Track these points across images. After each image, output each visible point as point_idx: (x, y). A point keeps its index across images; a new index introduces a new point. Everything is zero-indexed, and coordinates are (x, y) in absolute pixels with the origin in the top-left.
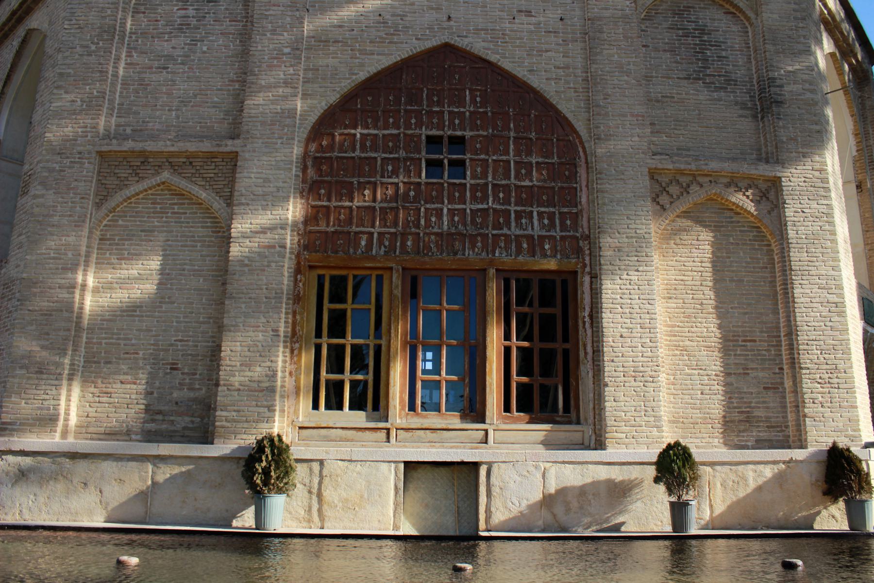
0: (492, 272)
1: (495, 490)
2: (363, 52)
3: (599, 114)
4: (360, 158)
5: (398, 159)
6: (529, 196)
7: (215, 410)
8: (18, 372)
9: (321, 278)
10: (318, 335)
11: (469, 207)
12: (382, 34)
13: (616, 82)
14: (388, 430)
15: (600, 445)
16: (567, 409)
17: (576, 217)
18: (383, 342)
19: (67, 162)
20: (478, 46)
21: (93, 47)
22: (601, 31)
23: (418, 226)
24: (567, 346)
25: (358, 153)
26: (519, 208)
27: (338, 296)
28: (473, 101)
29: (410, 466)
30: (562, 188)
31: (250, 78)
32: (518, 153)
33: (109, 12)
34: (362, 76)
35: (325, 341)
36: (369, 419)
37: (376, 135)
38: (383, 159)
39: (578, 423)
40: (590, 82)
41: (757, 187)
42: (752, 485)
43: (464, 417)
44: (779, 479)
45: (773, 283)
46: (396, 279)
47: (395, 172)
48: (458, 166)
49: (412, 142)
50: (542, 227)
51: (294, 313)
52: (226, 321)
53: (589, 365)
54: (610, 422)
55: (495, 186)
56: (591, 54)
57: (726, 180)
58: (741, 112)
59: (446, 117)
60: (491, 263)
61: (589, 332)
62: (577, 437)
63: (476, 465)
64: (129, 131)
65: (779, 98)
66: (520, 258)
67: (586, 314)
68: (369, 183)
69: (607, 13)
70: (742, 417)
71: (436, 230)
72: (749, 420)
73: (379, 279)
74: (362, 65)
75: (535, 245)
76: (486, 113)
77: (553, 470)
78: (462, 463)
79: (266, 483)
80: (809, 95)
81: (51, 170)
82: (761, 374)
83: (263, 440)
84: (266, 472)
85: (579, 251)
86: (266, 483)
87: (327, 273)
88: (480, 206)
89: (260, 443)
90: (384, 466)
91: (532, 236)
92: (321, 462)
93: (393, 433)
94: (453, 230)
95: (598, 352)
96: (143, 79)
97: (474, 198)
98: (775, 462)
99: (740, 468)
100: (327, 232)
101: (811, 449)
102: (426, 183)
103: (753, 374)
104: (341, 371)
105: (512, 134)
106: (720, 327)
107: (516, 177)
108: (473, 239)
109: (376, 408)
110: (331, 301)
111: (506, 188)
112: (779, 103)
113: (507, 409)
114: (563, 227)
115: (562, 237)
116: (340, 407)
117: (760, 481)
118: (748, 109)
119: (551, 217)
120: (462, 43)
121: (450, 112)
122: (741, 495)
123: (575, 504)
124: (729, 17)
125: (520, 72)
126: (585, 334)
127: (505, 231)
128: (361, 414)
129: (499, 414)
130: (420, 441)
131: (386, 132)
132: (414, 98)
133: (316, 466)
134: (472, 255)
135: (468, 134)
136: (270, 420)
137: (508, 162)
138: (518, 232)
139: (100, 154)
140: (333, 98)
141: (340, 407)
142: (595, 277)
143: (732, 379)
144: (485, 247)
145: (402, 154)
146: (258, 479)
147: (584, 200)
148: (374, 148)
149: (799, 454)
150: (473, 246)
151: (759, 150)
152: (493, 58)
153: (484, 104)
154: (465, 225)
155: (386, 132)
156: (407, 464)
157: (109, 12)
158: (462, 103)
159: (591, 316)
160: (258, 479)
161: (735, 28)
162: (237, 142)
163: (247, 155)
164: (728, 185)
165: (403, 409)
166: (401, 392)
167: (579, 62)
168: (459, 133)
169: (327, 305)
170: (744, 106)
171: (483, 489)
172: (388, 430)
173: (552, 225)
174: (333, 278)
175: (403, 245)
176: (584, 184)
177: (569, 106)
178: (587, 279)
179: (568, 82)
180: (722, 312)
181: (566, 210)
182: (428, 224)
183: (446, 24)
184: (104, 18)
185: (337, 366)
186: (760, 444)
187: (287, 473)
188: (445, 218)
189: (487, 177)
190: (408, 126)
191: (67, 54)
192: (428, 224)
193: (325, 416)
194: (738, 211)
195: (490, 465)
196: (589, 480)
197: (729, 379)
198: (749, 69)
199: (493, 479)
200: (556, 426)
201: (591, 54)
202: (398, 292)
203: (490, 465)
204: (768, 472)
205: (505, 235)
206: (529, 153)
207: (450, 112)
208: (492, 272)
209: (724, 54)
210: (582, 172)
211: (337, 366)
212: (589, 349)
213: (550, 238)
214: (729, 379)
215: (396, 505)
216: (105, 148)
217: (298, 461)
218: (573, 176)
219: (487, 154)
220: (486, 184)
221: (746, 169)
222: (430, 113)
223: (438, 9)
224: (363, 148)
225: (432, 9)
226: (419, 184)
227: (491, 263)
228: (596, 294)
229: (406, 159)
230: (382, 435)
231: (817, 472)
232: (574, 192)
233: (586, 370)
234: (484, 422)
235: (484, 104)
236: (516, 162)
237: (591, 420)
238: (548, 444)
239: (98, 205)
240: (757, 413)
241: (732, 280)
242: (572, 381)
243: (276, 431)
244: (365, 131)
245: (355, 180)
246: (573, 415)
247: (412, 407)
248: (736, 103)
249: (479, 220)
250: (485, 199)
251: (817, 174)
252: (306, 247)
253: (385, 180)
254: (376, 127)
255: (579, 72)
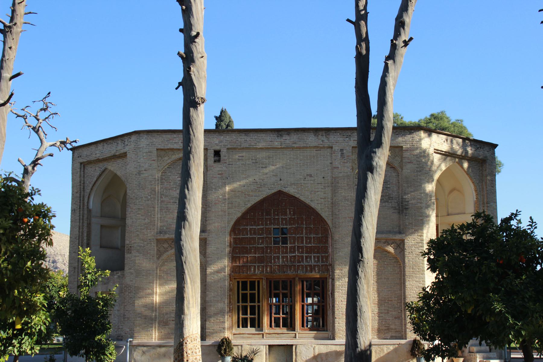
0: (297, 279)
1: (298, 354)
2: (249, 195)
3: (336, 218)
4: (250, 238)
5: (263, 238)
6: (310, 250)
7: (205, 329)
8: (138, 319)
9: (238, 282)
10: (238, 302)
11: (289, 255)
12: (256, 188)
13: (343, 204)
14: (263, 334)
15: (334, 339)
16: (323, 326)
17: (327, 258)
18: (260, 304)
19: (146, 243)
20: (291, 190)
21: (149, 197)
22: (338, 183)
23: (271, 263)
24: (323, 304)
25: (249, 236)
26: (307, 255)
27: (244, 288)
28: (290, 213)
29: (270, 346)
30: (322, 247)
31: (208, 209)
32: (306, 234)
33: (153, 182)
34: (249, 205)
35: (240, 304)
36: (256, 330)
37: (255, 229)
38: (258, 238)
39: (327, 331)
40: (333, 204)
41: (396, 243)
42: (386, 352)
43: (288, 330)
44: (395, 350)
45: (400, 279)
46: (264, 282)
47: (262, 243)
48: (285, 241)
49: (268, 231)
50: (315, 261)
51: (230, 295)
52: (207, 299)
53: (331, 311)
54: (337, 330)
55: (298, 247)
56: (334, 191)
57: (383, 241)
58: (393, 211)
59: (280, 220)
60: (297, 276)
61: (331, 299)
62: (326, 335)
63: (292, 345)
64: (165, 228)
65: (407, 207)
66: (307, 274)
67: (330, 293)
68: (253, 247)
69: (341, 175)
70: (386, 328)
71: (278, 264)
72: (388, 329)
73: (259, 282)
74: (249, 201)
75: (312, 268)
76: (295, 218)
77: (317, 347)
78: (287, 345)
79: (225, 353)
80: (419, 205)
81: (140, 246)
82: (394, 313)
83: (223, 339)
84: (225, 350)
85: (328, 270)
86: (225, 353)
87: (240, 280)
88: (293, 255)
89: (222, 340)
90: (262, 346)
91: (311, 265)
92: (242, 346)
93: (265, 335)
94: (283, 264)
95: (333, 306)
96: (167, 207)
97: (291, 252)
98: (394, 344)
99: (381, 346)
100: (239, 266)
101: (408, 340)
102: (274, 247)
103: (391, 313)
104: (247, 314)
105: (304, 226)
106: (378, 296)
107: (306, 243)
108: (290, 266)
109: (259, 326)
110: (242, 290)
111: (302, 248)
112: (406, 209)
113: (303, 326)
114: (322, 261)
115: (322, 265)
116: (247, 327)
117: (389, 351)
118: (396, 209)
119: (318, 257)
120: (285, 190)
121: (282, 218)
122: (382, 355)
123: (324, 358)
124: (392, 169)
125: (307, 201)
126: (330, 300)
127: (302, 264)
128: (254, 329)
129: (300, 328)
130: (273, 337)
131: (259, 227)
132: (268, 214)
133: (240, 347)
134: (290, 273)
135: (288, 227)
136: (224, 332)
137: (303, 237)
138: (306, 264)
139: (157, 239)
140: (239, 215)
141: (247, 327)
142: (333, 280)
143: (383, 315)
144: (295, 270)
145: (265, 235)
146: (223, 352)
147: (330, 251)
148: (255, 234)
149: (403, 342)
150: (290, 270)
151: (400, 226)
152: (297, 196)
153: (294, 214)
154: (287, 262)
155: (259, 227)
156: (269, 346)
157: (153, 182)
158: (286, 214)
159: (331, 294)
160: (223, 352)
161: (394, 174)
162: (206, 234)
163: (210, 239)
164: (385, 243)
165: (268, 327)
166: (267, 321)
167: (330, 195)
168: (285, 227)
169: (241, 292)
170: (395, 208)
171: (294, 353)
172: (263, 334)
173: (318, 260)
174: (242, 282)
175: (266, 270)
176: (330, 244)
177: (325, 214)
178: (330, 280)
179: (325, 205)
180: (379, 292)
181: (323, 255)
182: (275, 262)
183: (279, 182)
184: (152, 185)
185: (245, 313)
186: (392, 338)
187: (231, 350)
188: (281, 260)
189: (295, 244)
190: (266, 225)
191: (140, 200)
192: (275, 262)
193: (242, 330)
194: (389, 252)
195: (296, 345)
196: (329, 350)
197: (381, 315)
198: (398, 192)
199: (297, 350)
200: (319, 332)
201: (334, 191)
202: (265, 287)
203: (296, 345)
204: (392, 348)
205: (302, 265)
206: (310, 233)
207: (282, 218)
208: (297, 279)
209: (389, 186)
210: (330, 240)
211: (245, 313)
212: (331, 305)
213: (317, 265)
214: (381, 315)
215: (266, 359)
216: (159, 238)
217: (234, 345)
218: (326, 242)
219: (295, 234)
220: (295, 246)
221: (391, 237)
222: (274, 219)
223: (276, 176)
224: (251, 234)
225: (274, 176)
226: (271, 247)
227: (297, 276)
228: (333, 285)
229: (266, 238)
230: (261, 336)
231: (409, 348)
232: (327, 248)
233: (330, 312)
234: (295, 331)
235: (294, 214)
236: (306, 237)
237: (331, 330)
238: (316, 338)
239: (158, 258)
240: (391, 327)
241: (385, 278)
242: (325, 317)
243: (226, 336)
244: (251, 227)
245: (248, 246)
246: (325, 328)
247: (271, 326)
248: (392, 207)
249: (292, 260)
250: (294, 252)
251: (419, 237)
252: (232, 272)
253: (259, 246)
254: (255, 225)
255: (329, 200)
